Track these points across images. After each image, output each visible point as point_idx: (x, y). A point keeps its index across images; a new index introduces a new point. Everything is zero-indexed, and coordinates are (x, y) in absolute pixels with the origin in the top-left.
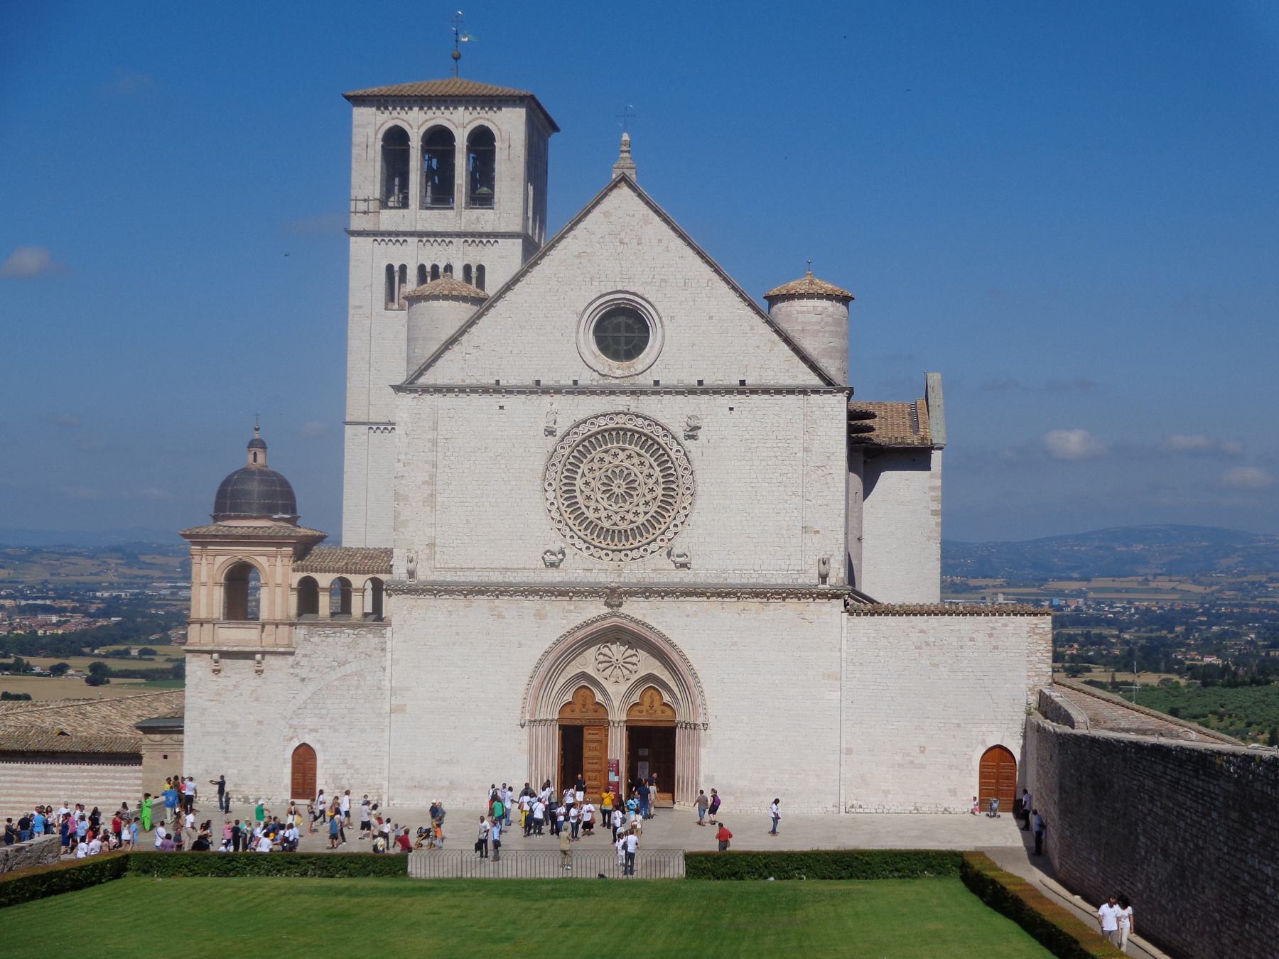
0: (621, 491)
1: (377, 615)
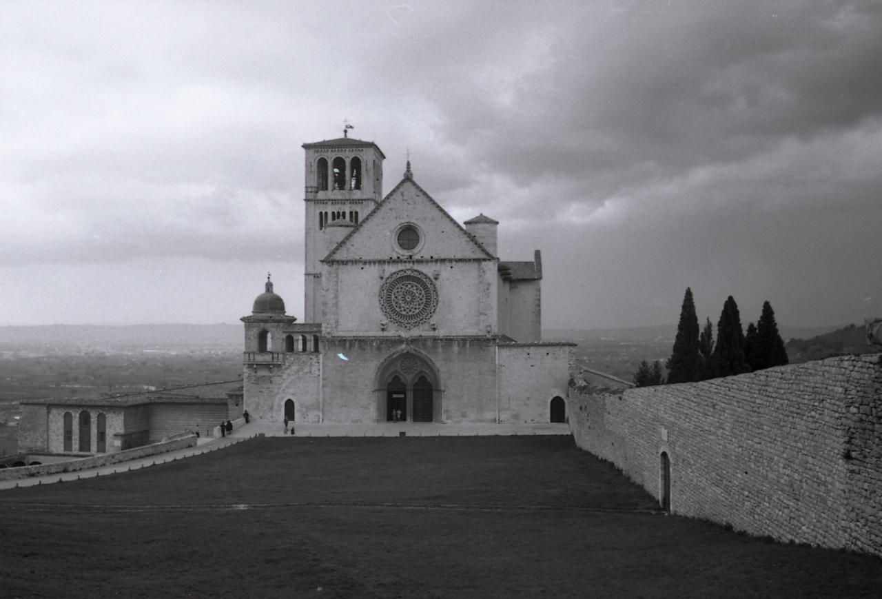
1: (316, 350)
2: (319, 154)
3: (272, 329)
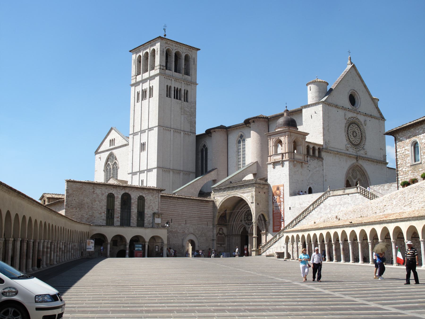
0: (355, 135)
2: (168, 45)
3: (301, 139)
